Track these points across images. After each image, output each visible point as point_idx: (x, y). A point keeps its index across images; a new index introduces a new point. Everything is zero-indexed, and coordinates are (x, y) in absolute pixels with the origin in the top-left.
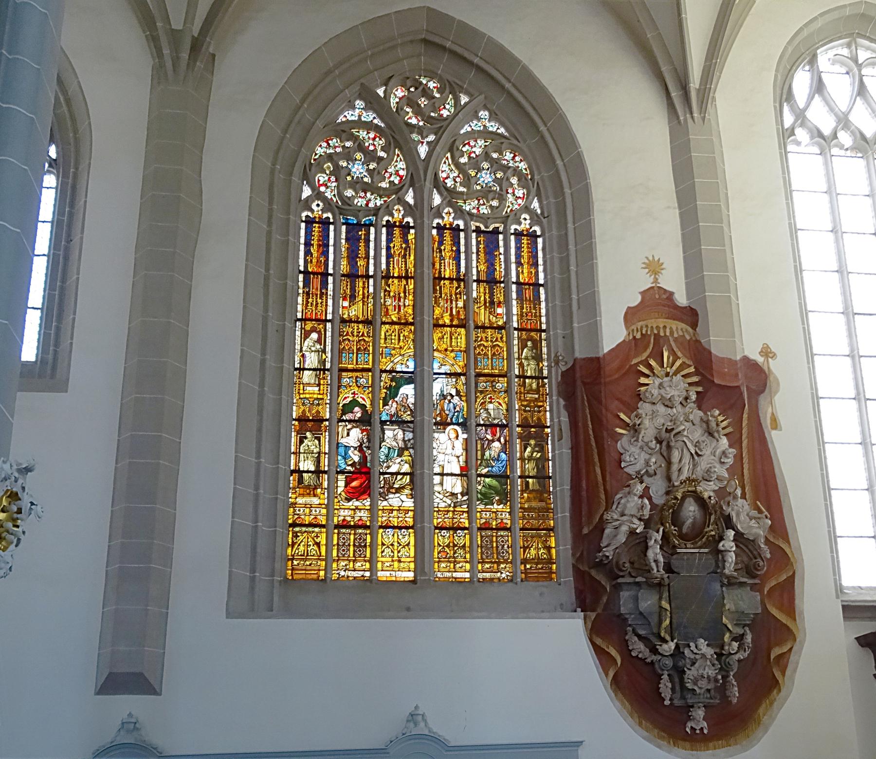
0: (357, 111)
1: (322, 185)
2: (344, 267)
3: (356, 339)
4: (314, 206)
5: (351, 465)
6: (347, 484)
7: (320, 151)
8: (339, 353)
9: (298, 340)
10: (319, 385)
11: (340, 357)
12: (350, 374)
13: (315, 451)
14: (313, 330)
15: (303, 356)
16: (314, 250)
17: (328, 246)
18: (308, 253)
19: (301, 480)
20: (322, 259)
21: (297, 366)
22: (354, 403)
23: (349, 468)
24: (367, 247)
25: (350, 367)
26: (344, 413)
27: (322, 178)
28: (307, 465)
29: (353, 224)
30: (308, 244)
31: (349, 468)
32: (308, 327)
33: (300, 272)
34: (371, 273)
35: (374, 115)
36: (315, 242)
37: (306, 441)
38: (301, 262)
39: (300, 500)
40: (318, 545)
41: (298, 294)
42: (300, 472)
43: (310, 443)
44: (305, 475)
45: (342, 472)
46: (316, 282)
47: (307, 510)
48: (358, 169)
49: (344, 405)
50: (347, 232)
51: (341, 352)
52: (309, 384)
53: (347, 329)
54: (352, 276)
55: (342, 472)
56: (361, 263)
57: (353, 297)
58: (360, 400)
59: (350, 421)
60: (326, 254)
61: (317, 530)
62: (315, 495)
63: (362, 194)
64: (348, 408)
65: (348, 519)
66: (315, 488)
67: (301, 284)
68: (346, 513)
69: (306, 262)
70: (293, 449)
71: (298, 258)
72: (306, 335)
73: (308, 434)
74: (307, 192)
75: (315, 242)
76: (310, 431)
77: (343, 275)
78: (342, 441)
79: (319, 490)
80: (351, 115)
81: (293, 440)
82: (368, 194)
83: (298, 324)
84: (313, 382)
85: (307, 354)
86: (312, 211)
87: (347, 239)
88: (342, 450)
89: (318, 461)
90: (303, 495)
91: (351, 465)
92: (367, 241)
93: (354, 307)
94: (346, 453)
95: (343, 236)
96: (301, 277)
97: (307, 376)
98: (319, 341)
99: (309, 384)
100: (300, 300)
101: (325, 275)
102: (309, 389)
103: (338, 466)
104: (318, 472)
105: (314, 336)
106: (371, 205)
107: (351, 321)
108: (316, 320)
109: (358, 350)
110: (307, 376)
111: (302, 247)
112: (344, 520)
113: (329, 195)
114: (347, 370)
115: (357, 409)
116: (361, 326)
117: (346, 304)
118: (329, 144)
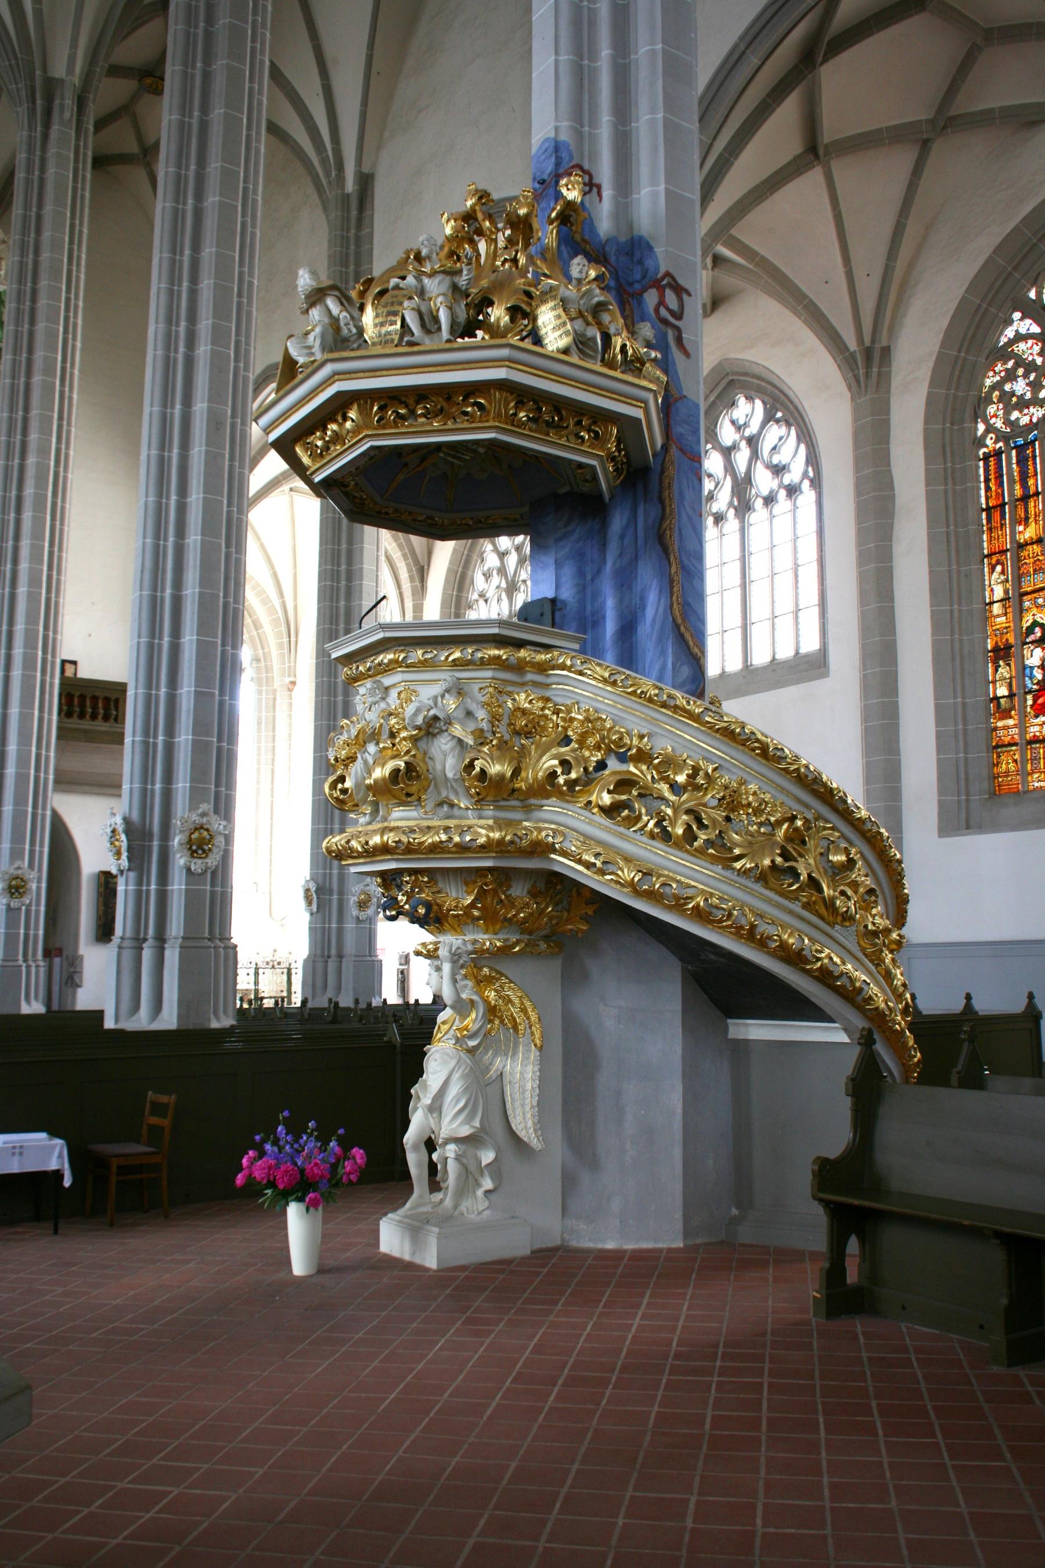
0: (1015, 323)
1: (991, 417)
2: (1018, 491)
3: (1032, 560)
4: (989, 442)
5: (1037, 684)
6: (1035, 700)
7: (988, 382)
8: (1018, 578)
9: (987, 578)
10: (1006, 614)
11: (1020, 582)
12: (1029, 597)
13: (1008, 676)
14: (998, 562)
15: (992, 590)
16: (992, 485)
17: (1002, 475)
18: (988, 489)
19: (999, 704)
20: (999, 491)
21: (988, 601)
22: (1035, 623)
23: (1035, 687)
24: (1035, 463)
25: (1029, 589)
26: (1027, 636)
27: (992, 409)
28: (1002, 691)
29: (1021, 445)
30: (987, 480)
31: (1035, 687)
32: (994, 561)
33: (983, 510)
34: (1040, 490)
35: (1030, 321)
36: (992, 477)
37: (1000, 669)
38: (983, 500)
39: (1000, 724)
40: (1015, 761)
41: (983, 532)
42: (996, 699)
43: (1004, 671)
44: (1002, 701)
45: (1030, 692)
46: (997, 516)
47: (1005, 732)
48: (1020, 387)
49: (1027, 628)
50: (1017, 456)
51: (1020, 577)
52: (998, 616)
53: (1024, 553)
54: (1025, 498)
55: (1030, 692)
56: (1031, 482)
57: (1027, 519)
58: (1039, 620)
59: (1032, 642)
60: (1000, 485)
61: (1014, 748)
62: (1011, 717)
63: (1026, 411)
64: (1030, 630)
65: (1038, 734)
66: (1010, 711)
67: (984, 522)
68: (1037, 728)
69: (987, 499)
70: (990, 678)
71: (979, 496)
72: (993, 569)
73: (1001, 663)
74: (981, 428)
75: (992, 477)
76: (1002, 659)
77: (1018, 500)
78: (1027, 662)
79: (1013, 712)
80: (1010, 333)
81: (990, 670)
82: (1031, 409)
83: (986, 560)
84: (1000, 612)
85: (994, 587)
86: (987, 446)
87: (1018, 463)
88: (1028, 671)
89: (1010, 686)
90: (1001, 719)
91: (1037, 684)
92: (1034, 457)
93: (1028, 529)
94: (1031, 673)
95: (1014, 461)
96: (984, 515)
97: (997, 608)
98: (1003, 572)
99: (998, 616)
100: (985, 537)
101: (1003, 505)
102: (998, 620)
103: (1025, 686)
104: (1011, 696)
105: (999, 568)
106: (1035, 420)
107: (1026, 544)
108: (999, 552)
109: (1035, 571)
110: (997, 608)
111: (982, 485)
112: (1035, 736)
113: (999, 424)
114: (1027, 593)
115: (1037, 629)
116: (1035, 547)
117: (1021, 528)
118: (995, 373)
